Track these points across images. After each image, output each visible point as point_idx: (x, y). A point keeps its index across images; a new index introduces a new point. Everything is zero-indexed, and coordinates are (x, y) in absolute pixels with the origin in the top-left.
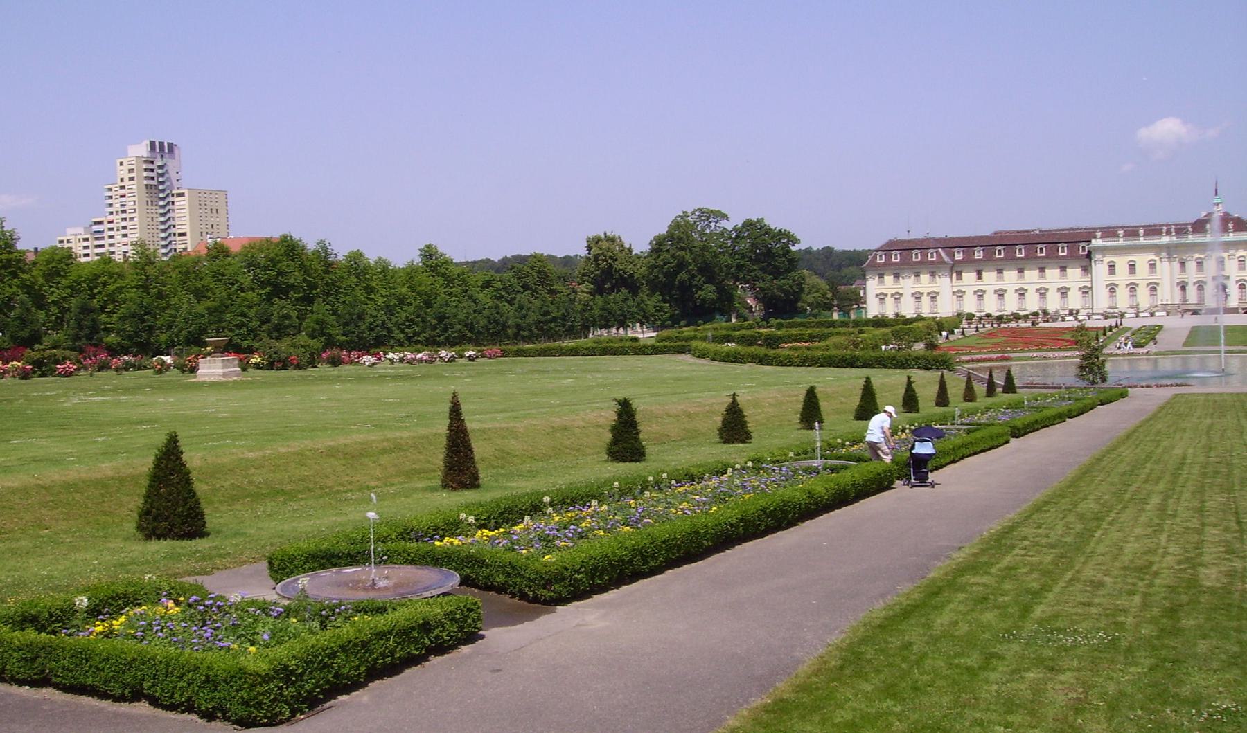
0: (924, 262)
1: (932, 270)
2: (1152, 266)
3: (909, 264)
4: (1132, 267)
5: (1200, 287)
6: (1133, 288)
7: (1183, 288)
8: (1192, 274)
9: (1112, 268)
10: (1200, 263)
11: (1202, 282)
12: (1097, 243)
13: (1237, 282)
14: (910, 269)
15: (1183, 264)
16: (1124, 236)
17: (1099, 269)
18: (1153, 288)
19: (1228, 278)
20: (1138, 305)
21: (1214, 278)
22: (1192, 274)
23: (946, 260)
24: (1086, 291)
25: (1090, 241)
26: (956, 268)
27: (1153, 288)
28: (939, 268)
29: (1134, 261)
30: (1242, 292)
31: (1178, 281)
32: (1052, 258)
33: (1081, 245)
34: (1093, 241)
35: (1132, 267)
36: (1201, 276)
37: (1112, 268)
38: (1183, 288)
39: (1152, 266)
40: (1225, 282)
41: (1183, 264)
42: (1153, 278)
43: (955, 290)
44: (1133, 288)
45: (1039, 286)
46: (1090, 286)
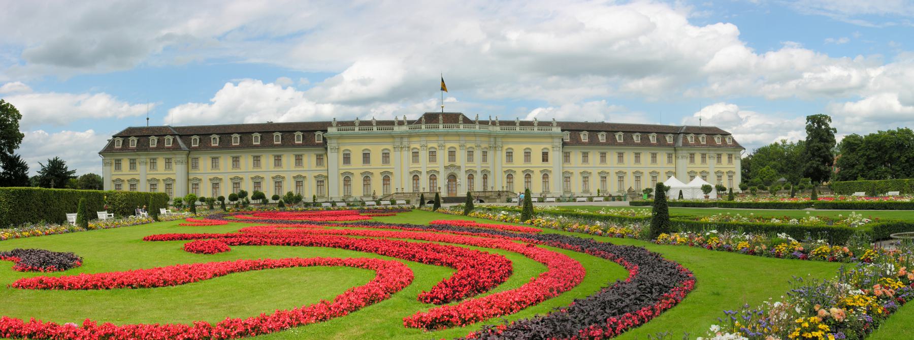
0: (160, 147)
1: (168, 157)
2: (386, 156)
3: (146, 150)
4: (366, 157)
5: (433, 178)
6: (367, 178)
7: (416, 178)
8: (424, 164)
9: (347, 159)
10: (433, 155)
11: (435, 171)
12: (332, 130)
13: (466, 172)
14: (147, 155)
15: (416, 155)
16: (359, 125)
17: (334, 158)
18: (386, 179)
19: (459, 167)
20: (374, 194)
21: (446, 167)
22: (424, 164)
23: (182, 146)
24: (321, 181)
25: (327, 130)
26: (191, 156)
27: (386, 179)
28: (175, 154)
29: (369, 150)
30: (471, 182)
31: (412, 170)
32: (288, 146)
33: (317, 133)
34: (329, 129)
35: (366, 157)
36: (433, 166)
37: (347, 159)
38: (416, 178)
39: (386, 156)
40: (456, 172)
41: (416, 155)
42: (386, 167)
43: (191, 177)
44: (367, 178)
45: (274, 175)
46: (325, 174)
